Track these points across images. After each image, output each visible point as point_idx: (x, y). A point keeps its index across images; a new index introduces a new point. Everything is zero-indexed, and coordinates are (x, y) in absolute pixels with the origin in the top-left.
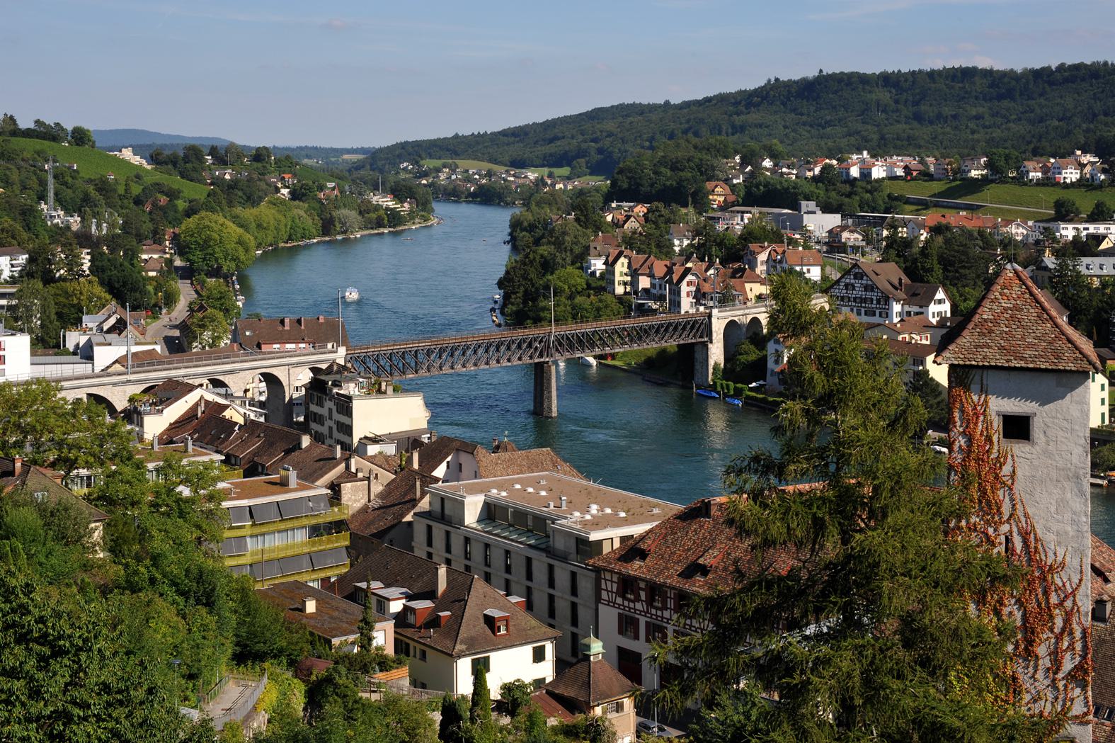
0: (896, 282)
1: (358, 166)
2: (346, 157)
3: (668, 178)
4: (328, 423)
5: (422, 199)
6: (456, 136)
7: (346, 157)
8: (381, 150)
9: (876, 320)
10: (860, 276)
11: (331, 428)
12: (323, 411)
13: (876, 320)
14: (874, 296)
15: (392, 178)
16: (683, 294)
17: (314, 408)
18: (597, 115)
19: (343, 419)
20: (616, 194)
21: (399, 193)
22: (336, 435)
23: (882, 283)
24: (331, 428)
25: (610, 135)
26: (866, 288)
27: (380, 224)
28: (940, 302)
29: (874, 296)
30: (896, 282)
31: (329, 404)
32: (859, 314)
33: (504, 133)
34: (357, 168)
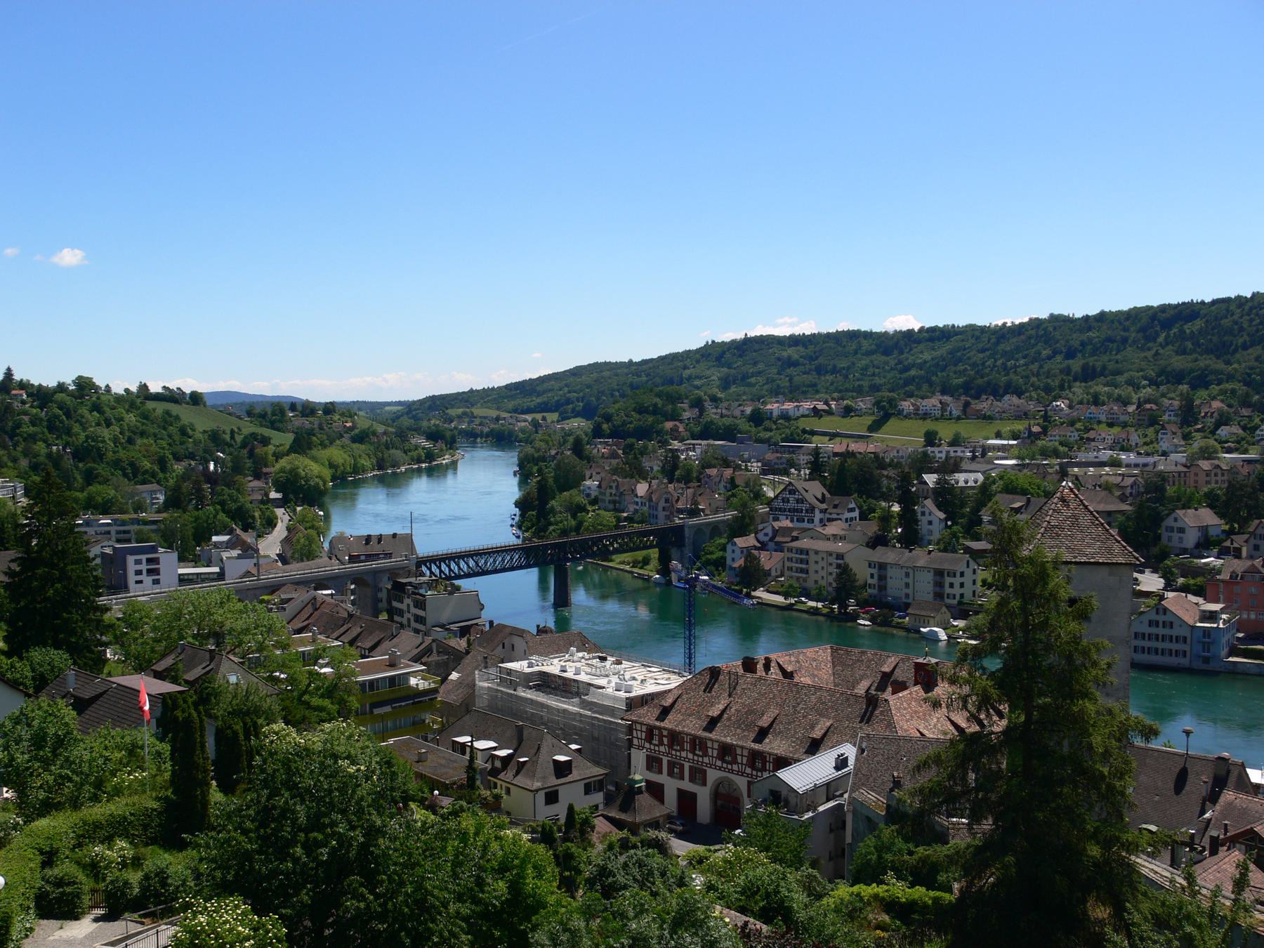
0: (820, 497)
1: (396, 417)
2: (388, 408)
3: (636, 420)
4: (407, 615)
5: (450, 442)
6: (471, 391)
7: (388, 408)
8: (414, 402)
9: (806, 525)
10: (793, 492)
11: (409, 620)
12: (403, 607)
13: (806, 525)
14: (804, 507)
15: (425, 424)
16: (660, 508)
17: (395, 604)
18: (577, 372)
19: (421, 613)
20: (597, 433)
21: (433, 436)
22: (413, 624)
23: (810, 498)
24: (409, 620)
25: (589, 386)
26: (798, 501)
27: (419, 461)
28: (852, 510)
29: (804, 507)
30: (820, 497)
31: (407, 601)
32: (792, 521)
33: (507, 387)
34: (398, 417)
